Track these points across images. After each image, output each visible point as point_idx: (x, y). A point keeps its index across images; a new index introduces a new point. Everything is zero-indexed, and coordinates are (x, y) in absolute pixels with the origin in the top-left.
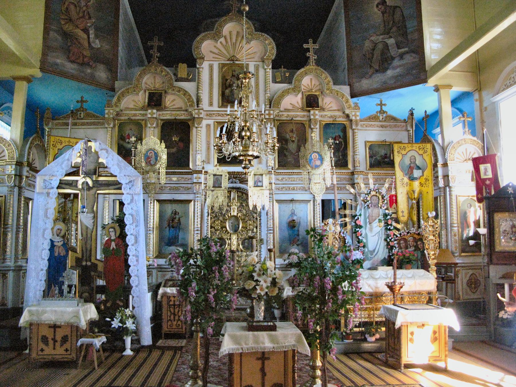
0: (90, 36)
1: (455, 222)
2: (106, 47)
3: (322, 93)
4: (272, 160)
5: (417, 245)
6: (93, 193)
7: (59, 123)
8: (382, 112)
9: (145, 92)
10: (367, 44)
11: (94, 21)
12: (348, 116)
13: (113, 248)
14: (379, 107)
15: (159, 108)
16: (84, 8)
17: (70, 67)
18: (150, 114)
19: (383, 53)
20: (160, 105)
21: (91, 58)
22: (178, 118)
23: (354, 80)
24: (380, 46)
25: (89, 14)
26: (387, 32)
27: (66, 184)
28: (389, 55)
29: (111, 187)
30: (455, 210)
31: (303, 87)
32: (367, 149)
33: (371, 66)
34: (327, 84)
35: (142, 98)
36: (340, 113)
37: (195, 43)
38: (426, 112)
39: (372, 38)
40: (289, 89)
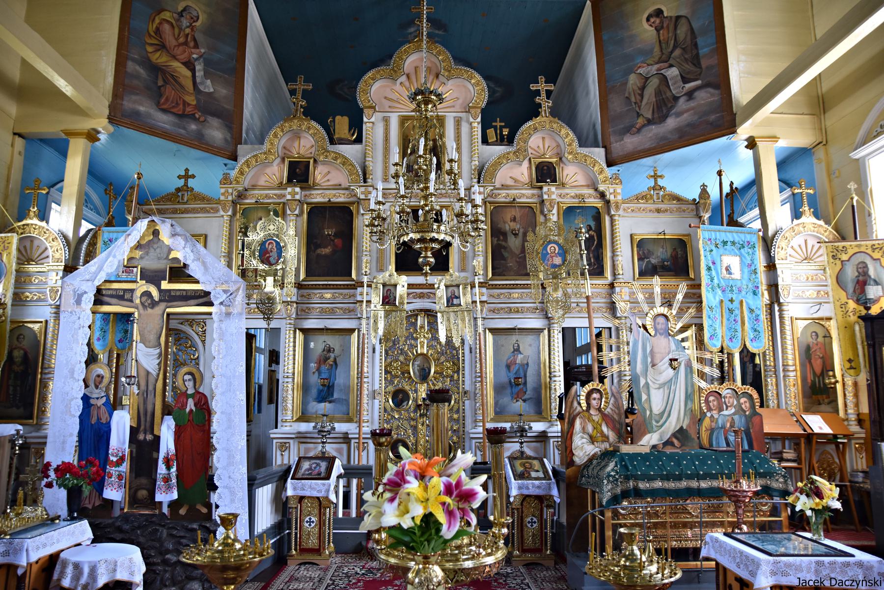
0: (197, 74)
1: (790, 362)
2: (223, 92)
3: (561, 159)
4: (480, 262)
5: (740, 405)
6: (160, 312)
8: (657, 188)
9: (283, 160)
10: (633, 80)
11: (203, 51)
12: (602, 195)
13: (191, 410)
14: (652, 180)
15: (304, 185)
16: (188, 31)
17: (164, 120)
18: (289, 193)
19: (658, 92)
20: (307, 180)
22: (333, 200)
23: (612, 139)
24: (654, 83)
25: (195, 40)
26: (666, 60)
27: (112, 296)
28: (669, 94)
29: (189, 302)
30: (789, 342)
31: (530, 151)
32: (635, 246)
33: (639, 115)
34: (570, 145)
35: (277, 171)
36: (591, 191)
37: (361, 85)
38: (732, 183)
39: (641, 71)
40: (508, 153)
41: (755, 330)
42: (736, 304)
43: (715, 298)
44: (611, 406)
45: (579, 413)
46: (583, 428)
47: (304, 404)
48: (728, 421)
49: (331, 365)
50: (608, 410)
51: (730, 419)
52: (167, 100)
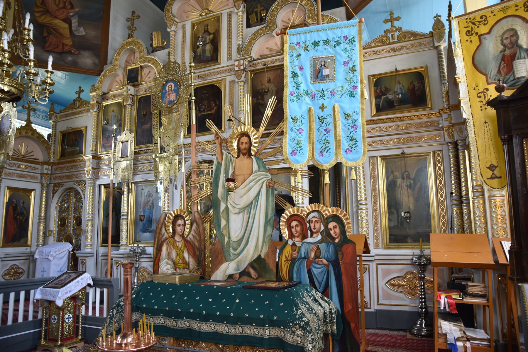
0: (73, 25)
7: (62, 116)
11: (77, 10)
15: (135, 83)
21: (73, 46)
32: (373, 85)
41: (352, 139)
42: (328, 111)
43: (300, 107)
44: (192, 232)
45: (166, 239)
46: (169, 254)
47: (136, 233)
48: (312, 250)
49: (150, 206)
50: (190, 236)
51: (315, 248)
52: (50, 44)
